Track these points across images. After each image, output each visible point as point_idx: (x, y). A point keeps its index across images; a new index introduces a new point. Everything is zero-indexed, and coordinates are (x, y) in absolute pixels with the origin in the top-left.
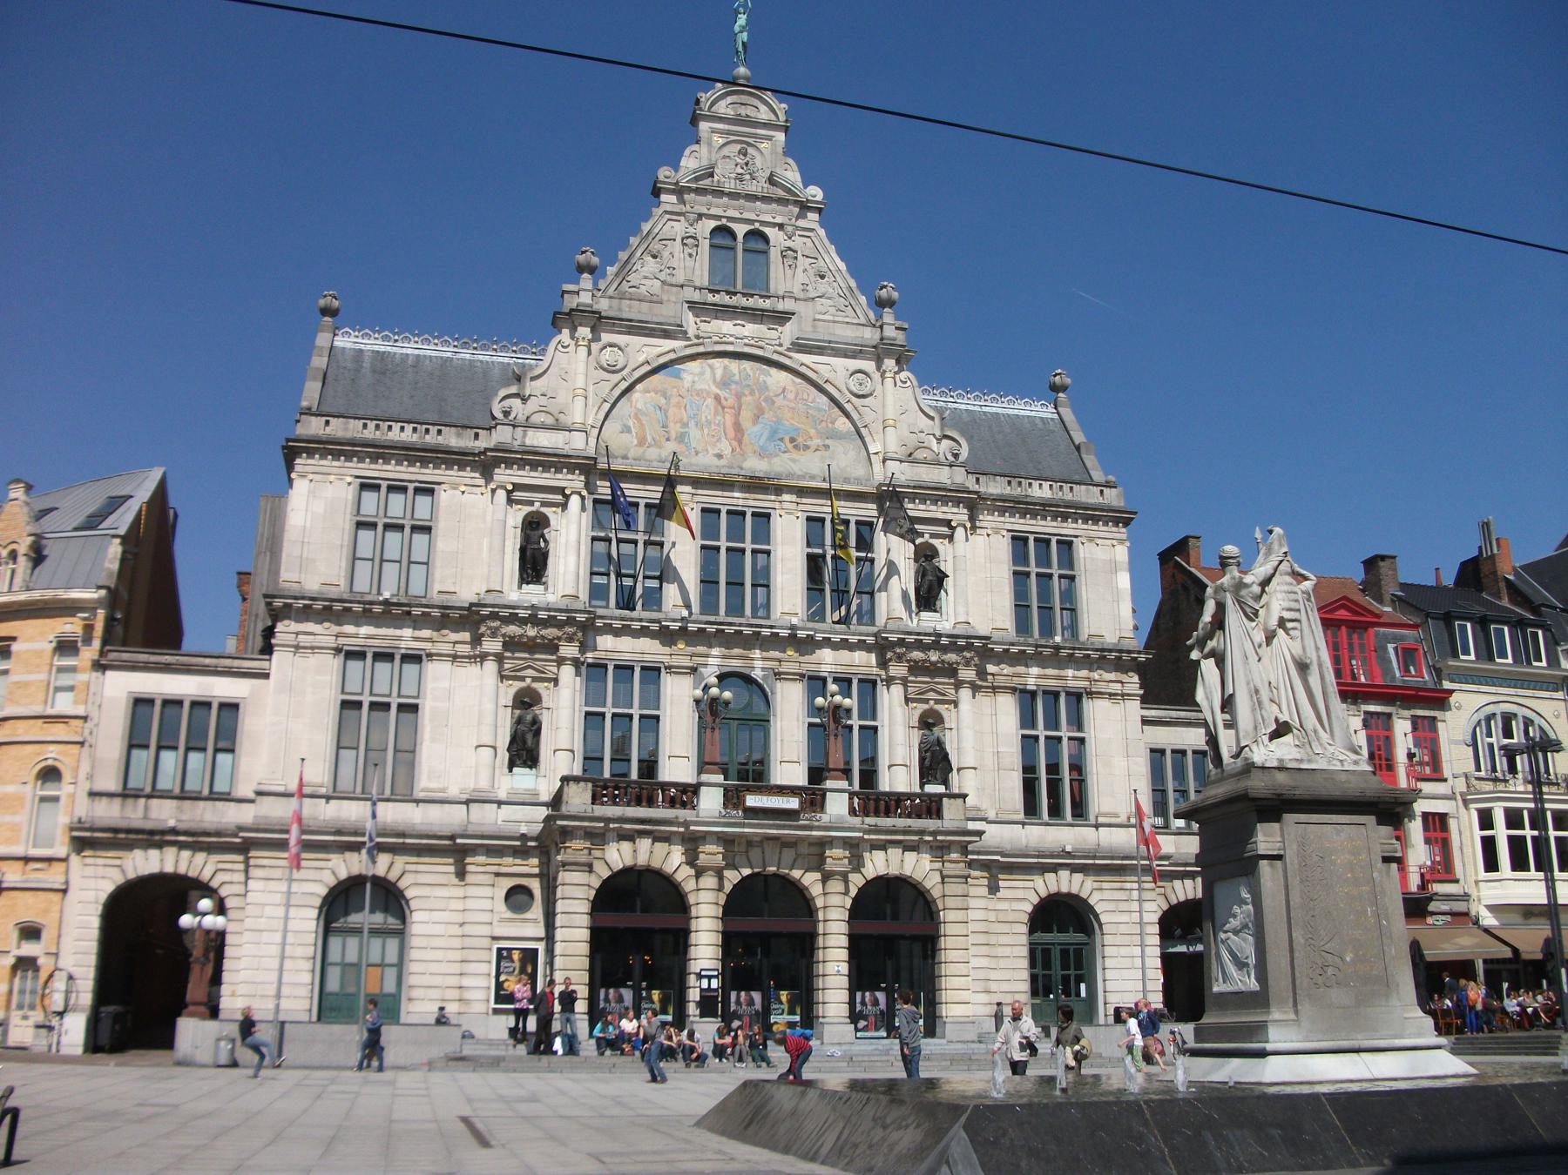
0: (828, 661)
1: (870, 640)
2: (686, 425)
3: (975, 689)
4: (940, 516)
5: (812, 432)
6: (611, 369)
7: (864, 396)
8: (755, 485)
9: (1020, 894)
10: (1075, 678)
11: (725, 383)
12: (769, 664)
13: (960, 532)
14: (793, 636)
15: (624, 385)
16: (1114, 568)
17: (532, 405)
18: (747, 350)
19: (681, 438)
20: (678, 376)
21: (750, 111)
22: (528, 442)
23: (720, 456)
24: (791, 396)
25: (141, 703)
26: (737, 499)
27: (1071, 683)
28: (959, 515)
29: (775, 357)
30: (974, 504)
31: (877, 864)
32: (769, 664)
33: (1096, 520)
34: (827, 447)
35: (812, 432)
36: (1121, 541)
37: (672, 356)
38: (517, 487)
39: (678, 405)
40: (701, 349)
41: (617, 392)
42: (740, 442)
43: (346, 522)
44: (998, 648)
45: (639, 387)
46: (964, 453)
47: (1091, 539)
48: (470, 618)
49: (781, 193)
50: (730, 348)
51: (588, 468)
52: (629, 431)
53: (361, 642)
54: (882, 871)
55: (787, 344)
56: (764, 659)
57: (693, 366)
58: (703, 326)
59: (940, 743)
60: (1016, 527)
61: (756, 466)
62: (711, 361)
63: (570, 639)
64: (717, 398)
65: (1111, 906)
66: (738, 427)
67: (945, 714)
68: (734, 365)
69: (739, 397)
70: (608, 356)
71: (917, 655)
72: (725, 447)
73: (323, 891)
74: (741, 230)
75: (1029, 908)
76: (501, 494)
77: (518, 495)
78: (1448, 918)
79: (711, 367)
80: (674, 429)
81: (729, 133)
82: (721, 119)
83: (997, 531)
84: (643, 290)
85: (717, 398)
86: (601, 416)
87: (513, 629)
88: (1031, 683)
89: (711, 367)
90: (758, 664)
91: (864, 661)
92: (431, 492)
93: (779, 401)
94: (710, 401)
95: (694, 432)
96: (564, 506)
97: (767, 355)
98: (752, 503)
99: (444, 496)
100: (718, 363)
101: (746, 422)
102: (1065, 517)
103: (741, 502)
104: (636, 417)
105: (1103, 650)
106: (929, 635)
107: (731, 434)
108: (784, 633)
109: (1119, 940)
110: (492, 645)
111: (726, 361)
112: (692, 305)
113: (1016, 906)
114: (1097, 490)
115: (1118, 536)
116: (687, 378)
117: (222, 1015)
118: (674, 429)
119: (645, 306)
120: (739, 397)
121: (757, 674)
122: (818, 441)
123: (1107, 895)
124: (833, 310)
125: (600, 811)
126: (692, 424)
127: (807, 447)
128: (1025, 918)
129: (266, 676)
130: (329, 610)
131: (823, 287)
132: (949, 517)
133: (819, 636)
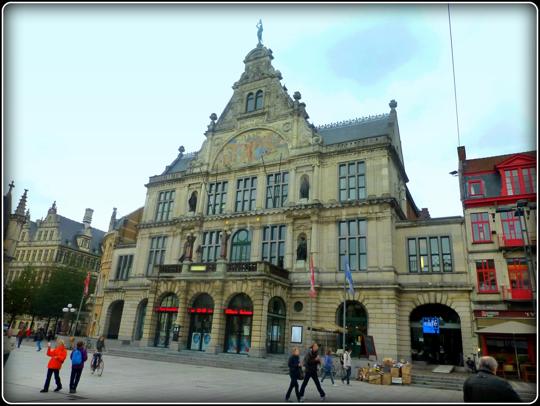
0: (270, 221)
1: (282, 212)
2: (236, 156)
3: (317, 222)
4: (308, 164)
5: (272, 147)
6: (218, 145)
7: (288, 131)
8: (251, 168)
9: (333, 301)
10: (361, 213)
11: (248, 140)
12: (252, 225)
13: (316, 168)
14: (256, 214)
15: (220, 149)
16: (381, 167)
17: (198, 161)
18: (254, 128)
19: (235, 160)
20: (236, 142)
21: (259, 56)
22: (194, 172)
23: (245, 163)
24: (267, 138)
25: (121, 257)
26: (248, 173)
27: (360, 216)
28: (315, 161)
29: (262, 127)
30: (321, 156)
31: (233, 288)
32: (252, 225)
33: (372, 150)
34: (276, 151)
35: (272, 147)
36: (384, 156)
37: (233, 136)
38: (190, 185)
39: (235, 151)
40: (241, 132)
41: (218, 151)
42: (251, 156)
43: (155, 204)
44: (328, 207)
45: (225, 148)
46: (321, 140)
47: (370, 158)
48: (174, 222)
49: (265, 75)
50: (249, 129)
51: (207, 174)
52: (221, 161)
53: (155, 234)
54: (235, 291)
55: (265, 121)
56: (250, 223)
57: (240, 138)
58: (242, 125)
59: (305, 245)
60: (341, 161)
61: (254, 162)
62: (245, 134)
63: (197, 226)
64: (246, 145)
65: (373, 306)
66: (251, 153)
67: (307, 234)
68: (251, 134)
69: (252, 143)
70: (216, 142)
71: (295, 213)
72: (247, 159)
73: (138, 303)
74: (255, 92)
75: (337, 307)
76: (186, 188)
77: (191, 187)
78: (497, 313)
79: (245, 136)
80: (233, 158)
81: (254, 64)
82: (251, 61)
83: (332, 164)
84: (228, 120)
85: (246, 145)
86: (214, 159)
87: (183, 225)
88: (344, 218)
89: (245, 136)
90: (249, 225)
91: (281, 219)
92: (174, 191)
93: (263, 141)
94: (244, 147)
95: (238, 157)
96: (201, 187)
97: (260, 127)
98: (251, 175)
99: (177, 191)
100: (246, 134)
101: (253, 150)
102: (359, 152)
103: (248, 175)
104: (224, 157)
105: (370, 201)
106: (298, 206)
107: (249, 154)
108: (254, 214)
109: (376, 321)
110: (179, 231)
111: (249, 133)
112: (238, 119)
113: (331, 306)
114: (374, 139)
115: (383, 154)
116: (238, 141)
117: (119, 338)
118: (233, 158)
119: (228, 124)
120: (252, 143)
121: (248, 229)
122: (274, 150)
123: (371, 301)
124: (281, 107)
125: (161, 275)
126: (238, 155)
127: (270, 153)
128: (335, 311)
129: (135, 247)
130: (148, 226)
131: (279, 100)
132: (312, 163)
133: (266, 213)
